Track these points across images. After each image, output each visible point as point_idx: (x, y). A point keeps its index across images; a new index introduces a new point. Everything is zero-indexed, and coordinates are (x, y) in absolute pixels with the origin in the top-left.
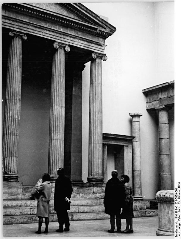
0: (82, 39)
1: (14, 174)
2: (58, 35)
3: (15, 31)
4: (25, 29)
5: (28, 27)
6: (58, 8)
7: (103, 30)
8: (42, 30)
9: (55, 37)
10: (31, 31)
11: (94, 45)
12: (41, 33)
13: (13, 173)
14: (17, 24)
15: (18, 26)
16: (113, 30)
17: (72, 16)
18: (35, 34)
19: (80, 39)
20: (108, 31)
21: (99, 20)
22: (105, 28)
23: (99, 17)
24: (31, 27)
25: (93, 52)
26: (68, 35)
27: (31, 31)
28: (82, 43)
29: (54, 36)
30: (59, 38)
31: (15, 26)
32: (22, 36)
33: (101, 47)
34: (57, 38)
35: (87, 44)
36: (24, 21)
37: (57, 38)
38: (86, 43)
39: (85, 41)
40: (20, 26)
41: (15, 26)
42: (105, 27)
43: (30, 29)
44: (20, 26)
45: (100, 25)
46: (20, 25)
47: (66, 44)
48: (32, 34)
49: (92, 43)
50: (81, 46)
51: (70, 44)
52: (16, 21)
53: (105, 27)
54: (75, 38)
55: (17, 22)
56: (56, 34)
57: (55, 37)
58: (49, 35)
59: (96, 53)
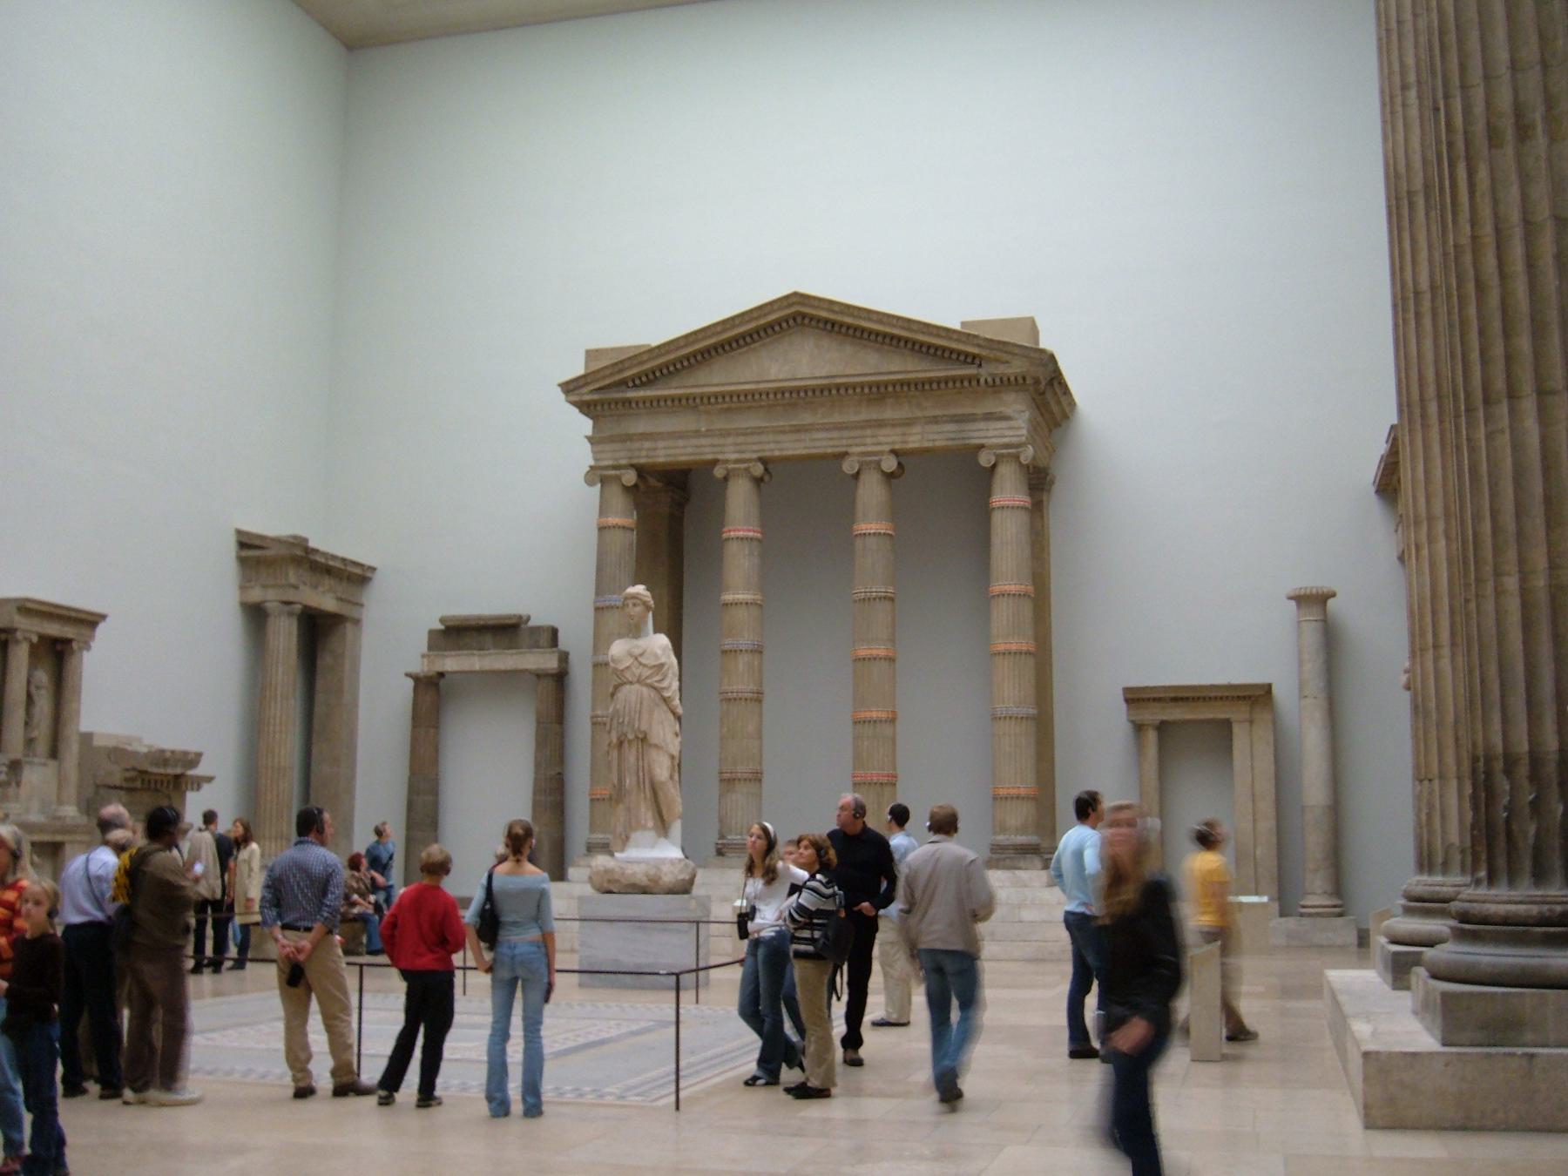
0: (935, 420)
2: (853, 434)
3: (727, 461)
4: (755, 448)
5: (763, 438)
10: (772, 446)
11: (981, 425)
14: (730, 440)
18: (785, 453)
21: (979, 346)
24: (771, 437)
25: (982, 446)
27: (772, 446)
30: (857, 441)
32: (747, 469)
33: (1011, 423)
38: (952, 427)
42: (1005, 357)
45: (989, 360)
46: (741, 439)
47: (882, 453)
48: (777, 453)
49: (974, 420)
51: (897, 447)
52: (726, 433)
53: (1005, 357)
56: (846, 434)
59: (991, 447)
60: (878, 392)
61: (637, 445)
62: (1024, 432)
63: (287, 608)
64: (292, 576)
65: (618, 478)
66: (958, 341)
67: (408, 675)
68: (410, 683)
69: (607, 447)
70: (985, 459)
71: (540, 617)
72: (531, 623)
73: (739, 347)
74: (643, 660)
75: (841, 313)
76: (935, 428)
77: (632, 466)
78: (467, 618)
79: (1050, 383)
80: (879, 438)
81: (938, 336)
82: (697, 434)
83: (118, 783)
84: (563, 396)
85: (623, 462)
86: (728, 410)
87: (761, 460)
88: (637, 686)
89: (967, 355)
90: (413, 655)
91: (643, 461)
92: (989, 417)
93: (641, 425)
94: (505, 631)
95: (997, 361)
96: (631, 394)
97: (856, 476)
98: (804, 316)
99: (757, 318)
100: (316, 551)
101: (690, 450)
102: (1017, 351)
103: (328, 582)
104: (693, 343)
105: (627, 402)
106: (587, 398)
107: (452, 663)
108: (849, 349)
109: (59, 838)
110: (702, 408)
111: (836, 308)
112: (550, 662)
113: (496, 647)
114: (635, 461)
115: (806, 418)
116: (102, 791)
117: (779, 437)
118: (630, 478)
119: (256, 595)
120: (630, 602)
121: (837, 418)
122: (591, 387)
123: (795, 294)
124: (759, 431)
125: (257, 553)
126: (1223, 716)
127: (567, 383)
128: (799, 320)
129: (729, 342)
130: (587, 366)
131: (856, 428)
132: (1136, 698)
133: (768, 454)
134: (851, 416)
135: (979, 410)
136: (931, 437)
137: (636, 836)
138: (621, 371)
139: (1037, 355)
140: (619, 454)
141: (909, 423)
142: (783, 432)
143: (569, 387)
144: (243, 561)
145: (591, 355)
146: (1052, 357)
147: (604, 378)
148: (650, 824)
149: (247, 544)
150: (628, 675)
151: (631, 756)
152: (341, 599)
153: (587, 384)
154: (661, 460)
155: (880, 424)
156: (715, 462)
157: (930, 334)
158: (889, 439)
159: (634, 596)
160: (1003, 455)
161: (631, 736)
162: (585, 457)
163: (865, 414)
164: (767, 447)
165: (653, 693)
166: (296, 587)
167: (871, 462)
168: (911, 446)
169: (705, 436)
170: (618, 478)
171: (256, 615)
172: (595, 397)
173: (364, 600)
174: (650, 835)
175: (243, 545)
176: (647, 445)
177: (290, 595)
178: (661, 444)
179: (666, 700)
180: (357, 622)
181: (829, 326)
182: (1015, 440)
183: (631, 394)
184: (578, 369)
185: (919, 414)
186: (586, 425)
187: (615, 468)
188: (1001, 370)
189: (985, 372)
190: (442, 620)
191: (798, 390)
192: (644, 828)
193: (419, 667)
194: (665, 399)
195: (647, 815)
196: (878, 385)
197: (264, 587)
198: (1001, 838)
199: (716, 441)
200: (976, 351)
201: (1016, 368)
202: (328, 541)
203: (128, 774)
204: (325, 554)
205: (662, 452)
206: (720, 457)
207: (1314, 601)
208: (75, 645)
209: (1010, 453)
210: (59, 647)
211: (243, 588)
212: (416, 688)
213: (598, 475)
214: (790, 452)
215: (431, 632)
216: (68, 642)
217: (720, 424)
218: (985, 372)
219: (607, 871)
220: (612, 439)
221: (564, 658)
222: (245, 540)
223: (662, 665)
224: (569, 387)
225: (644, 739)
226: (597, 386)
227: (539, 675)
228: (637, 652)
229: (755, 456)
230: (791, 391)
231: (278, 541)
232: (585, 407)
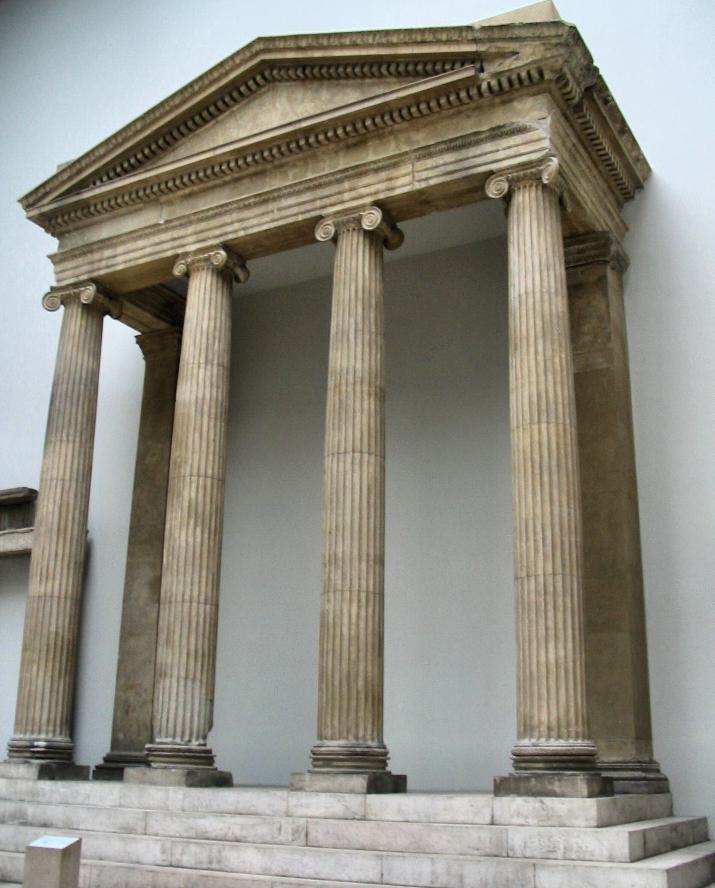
0: (426, 152)
1: (169, 740)
3: (186, 254)
5: (227, 219)
6: (323, 98)
7: (508, 64)
8: (271, 206)
9: (318, 204)
10: (237, 226)
11: (488, 147)
13: (167, 737)
14: (191, 229)
15: (197, 233)
17: (352, 96)
18: (250, 231)
19: (419, 159)
20: (533, 53)
21: (475, 41)
22: (515, 53)
23: (469, 28)
24: (235, 216)
25: (491, 173)
26: (364, 169)
27: (237, 226)
28: (434, 164)
29: (313, 200)
31: (185, 241)
32: (207, 259)
33: (528, 136)
34: (326, 201)
35: (453, 160)
36: (208, 210)
37: (326, 201)
38: (449, 157)
39: (441, 152)
40: (202, 232)
41: (185, 241)
43: (232, 223)
44: (202, 232)
46: (203, 225)
47: (363, 207)
48: (242, 233)
49: (478, 143)
50: (427, 179)
51: (382, 196)
52: (186, 221)
54: (395, 165)
55: (190, 223)
56: (319, 193)
58: (296, 210)
59: (500, 172)
60: (353, 132)
62: (546, 143)
75: (310, 48)
76: (430, 162)
77: (93, 280)
79: (588, 90)
81: (424, 43)
82: (155, 229)
87: (226, 246)
91: (102, 272)
92: (498, 133)
95: (503, 55)
96: (86, 195)
97: (335, 240)
98: (272, 65)
101: (148, 250)
102: (524, 33)
105: (84, 205)
106: (45, 209)
110: (164, 199)
111: (303, 44)
114: (95, 274)
115: (274, 183)
117: (246, 214)
123: (260, 40)
124: (222, 210)
127: (27, 197)
131: (330, 184)
133: (231, 236)
136: (425, 175)
138: (79, 172)
139: (553, 32)
140: (80, 270)
141: (394, 162)
142: (248, 207)
145: (59, 166)
146: (574, 33)
147: (64, 183)
155: (359, 172)
158: (372, 189)
160: (518, 180)
162: (47, 277)
163: (343, 162)
164: (229, 229)
167: (350, 220)
168: (398, 192)
169: (167, 230)
176: (108, 253)
178: (120, 249)
182: (534, 157)
183: (86, 195)
188: (508, 64)
198: (528, 744)
199: (176, 233)
201: (528, 55)
206: (180, 251)
209: (526, 175)
214: (255, 230)
224: (30, 201)
232: (48, 222)
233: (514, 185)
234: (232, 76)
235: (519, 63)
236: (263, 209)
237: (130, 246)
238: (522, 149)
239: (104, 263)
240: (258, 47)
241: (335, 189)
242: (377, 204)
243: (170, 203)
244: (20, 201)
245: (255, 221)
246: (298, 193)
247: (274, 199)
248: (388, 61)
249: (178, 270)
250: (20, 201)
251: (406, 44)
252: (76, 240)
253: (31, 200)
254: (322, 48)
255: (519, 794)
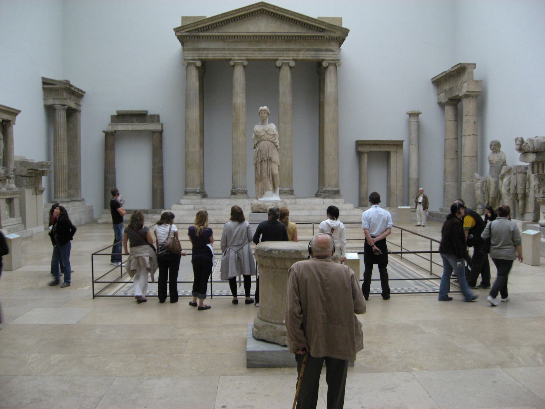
0: (308, 50)
3: (235, 60)
5: (248, 52)
8: (262, 52)
9: (277, 55)
10: (251, 55)
11: (324, 53)
12: (262, 55)
14: (236, 52)
16: (346, 32)
21: (325, 26)
24: (251, 52)
25: (323, 60)
27: (251, 55)
32: (242, 63)
33: (334, 53)
38: (313, 53)
39: (312, 51)
42: (334, 30)
45: (328, 31)
46: (239, 52)
47: (290, 60)
48: (253, 58)
51: (295, 58)
52: (235, 50)
53: (334, 30)
56: (277, 52)
57: (277, 55)
59: (327, 60)
60: (289, 39)
61: (201, 52)
63: (63, 107)
64: (65, 95)
65: (195, 64)
66: (319, 24)
67: (104, 132)
68: (104, 134)
69: (190, 52)
70: (325, 64)
71: (151, 112)
72: (149, 113)
73: (240, 19)
74: (269, 132)
75: (278, 10)
76: (309, 53)
77: (199, 59)
78: (127, 111)
80: (288, 56)
81: (312, 21)
82: (224, 49)
83: (26, 175)
84: (174, 33)
85: (196, 58)
86: (236, 42)
87: (247, 60)
88: (267, 142)
89: (320, 28)
90: (104, 123)
91: (204, 58)
92: (327, 50)
93: (203, 45)
94: (141, 116)
95: (331, 31)
96: (201, 34)
98: (264, 10)
99: (248, 10)
100: (72, 86)
101: (221, 55)
103: (73, 97)
104: (224, 17)
105: (199, 37)
107: (121, 127)
108: (279, 23)
109: (12, 196)
112: (158, 128)
113: (137, 122)
114: (201, 58)
115: (264, 46)
116: (18, 178)
117: (254, 52)
118: (199, 64)
119: (50, 102)
120: (263, 112)
121: (274, 47)
122: (186, 30)
123: (262, 2)
125: (52, 86)
126: (387, 150)
128: (262, 11)
129: (236, 17)
130: (182, 23)
132: (359, 144)
133: (249, 58)
134: (279, 47)
135: (324, 48)
137: (267, 193)
138: (198, 25)
141: (299, 50)
142: (255, 51)
143: (177, 30)
144: (44, 89)
145: (184, 19)
148: (271, 189)
149: (46, 83)
150: (263, 137)
151: (265, 165)
152: (76, 104)
153: (183, 29)
154: (211, 58)
155: (289, 50)
156: (230, 60)
157: (309, 20)
158: (293, 55)
159: (265, 110)
161: (266, 159)
163: (284, 46)
164: (248, 55)
165: (273, 144)
166: (66, 99)
168: (299, 58)
170: (195, 64)
171: (50, 110)
172: (187, 34)
173: (81, 103)
174: (271, 192)
175: (44, 83)
176: (205, 52)
177: (65, 102)
178: (210, 52)
179: (276, 146)
180: (80, 111)
181: (272, 15)
183: (201, 34)
184: (179, 24)
185: (302, 47)
186: (178, 45)
187: (193, 60)
189: (326, 35)
190: (117, 112)
191: (262, 36)
192: (269, 190)
193: (110, 129)
194: (213, 36)
195: (270, 186)
196: (290, 36)
197: (54, 99)
200: (324, 27)
202: (76, 83)
203: (29, 171)
204: (76, 88)
205: (211, 55)
206: (232, 58)
207: (414, 115)
208: (11, 122)
210: (4, 123)
211: (45, 99)
212: (106, 136)
213: (188, 64)
214: (257, 58)
215: (112, 116)
216: (8, 121)
217: (232, 46)
218: (326, 35)
219: (258, 205)
220: (192, 50)
221: (162, 125)
222: (45, 81)
223: (275, 135)
224: (177, 30)
225: (270, 160)
226: (188, 30)
227: (154, 132)
228: (267, 130)
229: (245, 58)
230: (259, 36)
231: (60, 82)
233: (330, 64)
234: (252, 10)
235: (335, 35)
236: (259, 52)
237: (214, 52)
238: (332, 56)
239: (204, 55)
240: (261, 4)
241: (282, 53)
242: (293, 60)
243: (228, 42)
244: (174, 29)
245: (257, 55)
246: (272, 51)
247: (264, 51)
248: (300, 22)
249: (232, 63)
250: (174, 29)
251: (307, 20)
252: (190, 45)
253: (178, 30)
254: (282, 12)
255: (329, 198)
